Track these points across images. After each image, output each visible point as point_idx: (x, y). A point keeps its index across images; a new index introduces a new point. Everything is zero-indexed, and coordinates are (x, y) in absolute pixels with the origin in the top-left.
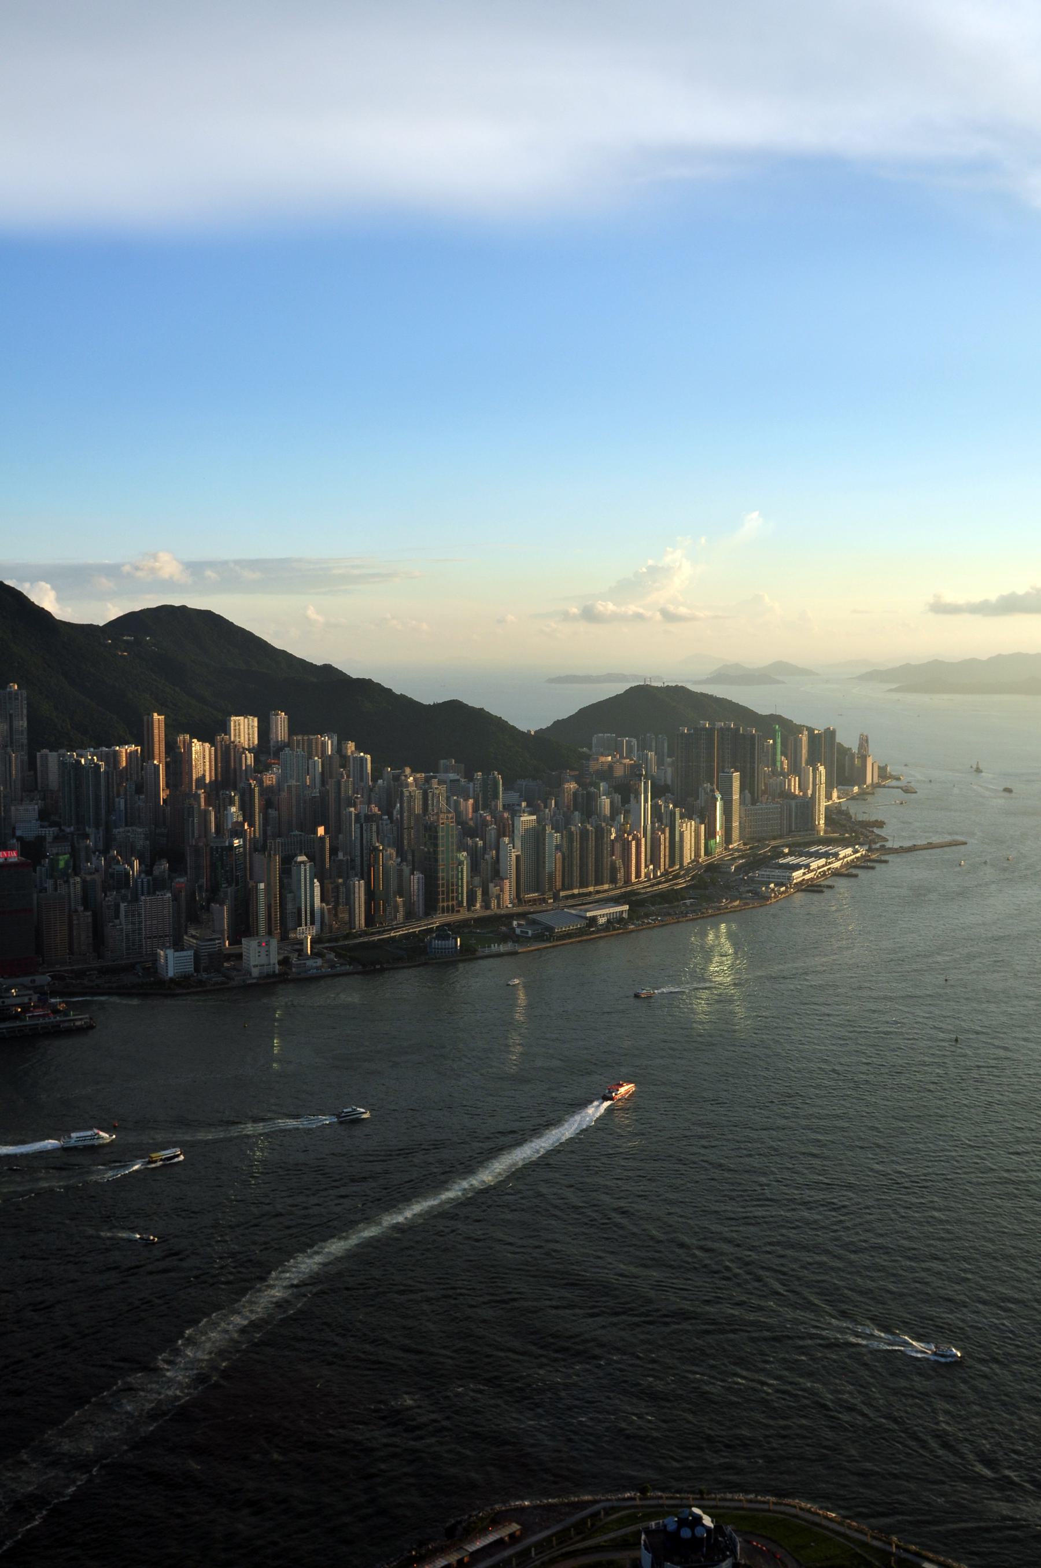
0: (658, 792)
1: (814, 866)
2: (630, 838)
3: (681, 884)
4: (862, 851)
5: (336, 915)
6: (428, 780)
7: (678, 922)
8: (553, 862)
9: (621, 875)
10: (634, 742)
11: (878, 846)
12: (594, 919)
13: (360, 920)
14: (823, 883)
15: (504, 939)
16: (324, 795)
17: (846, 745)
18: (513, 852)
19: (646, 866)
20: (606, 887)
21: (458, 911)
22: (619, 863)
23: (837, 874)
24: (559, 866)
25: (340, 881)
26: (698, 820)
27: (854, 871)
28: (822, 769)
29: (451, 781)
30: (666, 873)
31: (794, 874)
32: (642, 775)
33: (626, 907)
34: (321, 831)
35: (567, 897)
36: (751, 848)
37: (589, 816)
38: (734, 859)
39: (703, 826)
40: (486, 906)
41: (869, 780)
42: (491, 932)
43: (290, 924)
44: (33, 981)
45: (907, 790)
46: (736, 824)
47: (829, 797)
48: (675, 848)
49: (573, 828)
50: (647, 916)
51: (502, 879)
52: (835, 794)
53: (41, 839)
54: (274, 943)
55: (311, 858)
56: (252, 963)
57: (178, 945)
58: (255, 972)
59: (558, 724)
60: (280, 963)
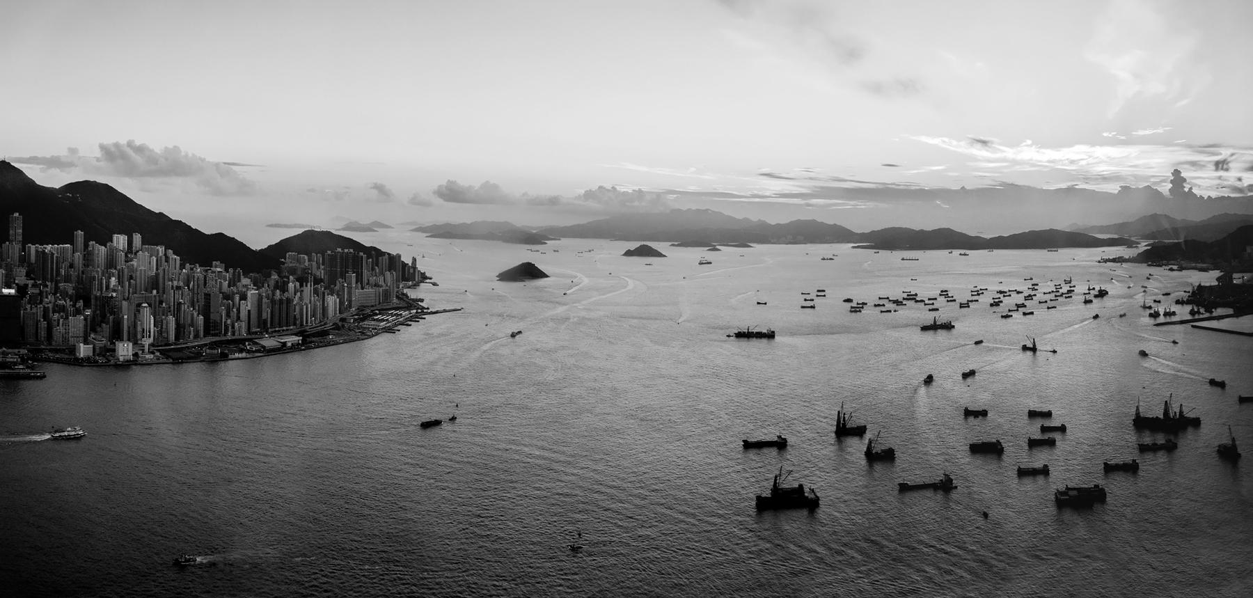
3: (328, 326)
5: (161, 334)
6: (206, 271)
8: (266, 314)
12: (284, 344)
13: (172, 337)
15: (241, 351)
16: (157, 275)
20: (292, 327)
24: (269, 316)
25: (164, 317)
29: (219, 272)
33: (301, 338)
34: (155, 292)
37: (284, 292)
40: (233, 334)
41: (417, 280)
42: (236, 347)
43: (139, 337)
44: (19, 352)
48: (324, 309)
50: (311, 342)
53: (27, 285)
54: (131, 344)
55: (150, 305)
56: (120, 354)
57: (86, 342)
58: (121, 359)
60: (133, 355)
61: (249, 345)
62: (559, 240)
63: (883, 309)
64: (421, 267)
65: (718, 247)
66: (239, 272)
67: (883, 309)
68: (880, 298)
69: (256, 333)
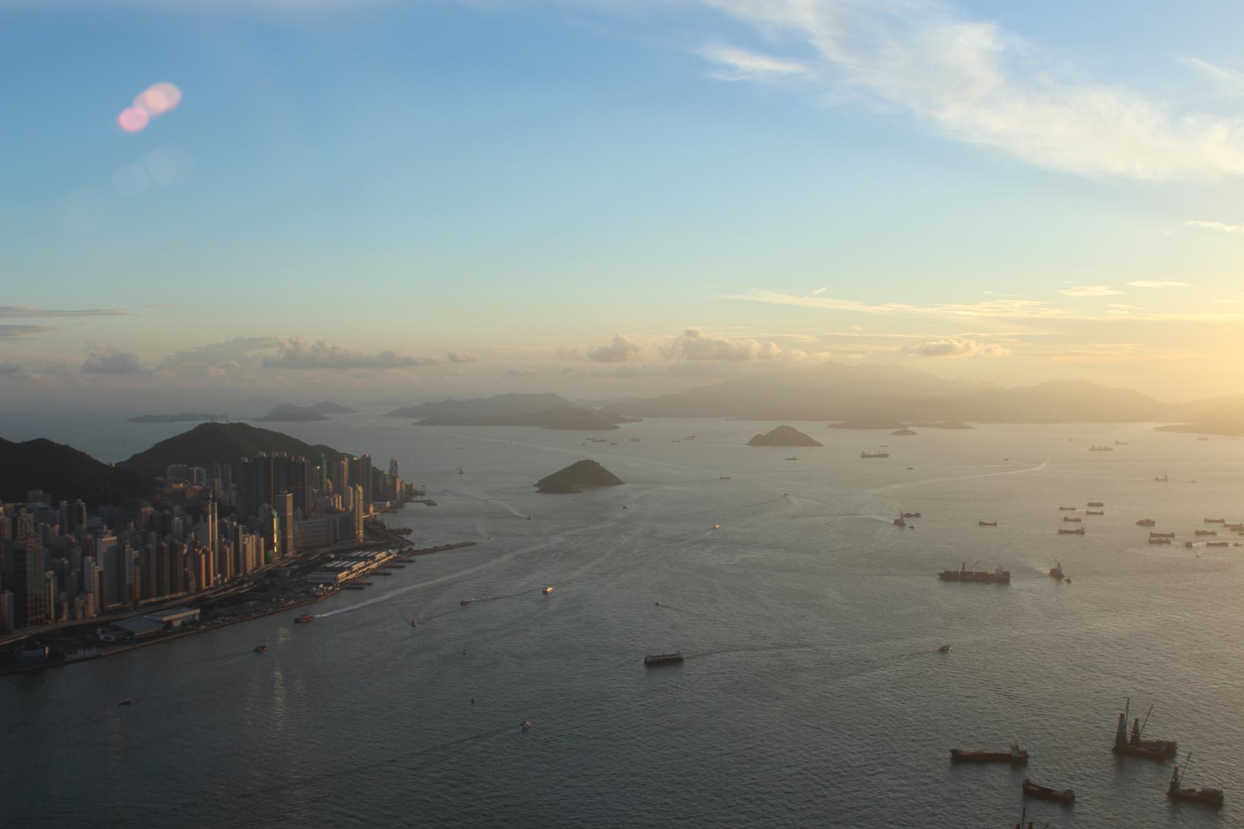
0: (224, 512)
1: (355, 567)
2: (200, 552)
4: (394, 553)
6: (17, 509)
7: (243, 621)
8: (132, 575)
9: (192, 584)
10: (203, 470)
11: (406, 549)
12: (169, 623)
14: (363, 582)
17: (380, 468)
18: (96, 568)
19: (215, 575)
20: (180, 594)
21: (46, 623)
22: (191, 574)
23: (374, 573)
26: (258, 535)
27: (388, 571)
28: (360, 489)
29: (40, 509)
30: (232, 580)
31: (339, 576)
32: (209, 498)
33: (198, 611)
35: (146, 605)
36: (303, 556)
38: (289, 566)
39: (262, 540)
40: (73, 616)
45: (429, 503)
46: (290, 536)
47: (366, 511)
49: (150, 546)
51: (87, 593)
52: (371, 509)
59: (136, 456)
61: (103, 632)
62: (641, 421)
63: (1212, 540)
64: (403, 479)
65: (911, 429)
66: (80, 510)
67: (1212, 540)
68: (1207, 521)
69: (117, 611)
